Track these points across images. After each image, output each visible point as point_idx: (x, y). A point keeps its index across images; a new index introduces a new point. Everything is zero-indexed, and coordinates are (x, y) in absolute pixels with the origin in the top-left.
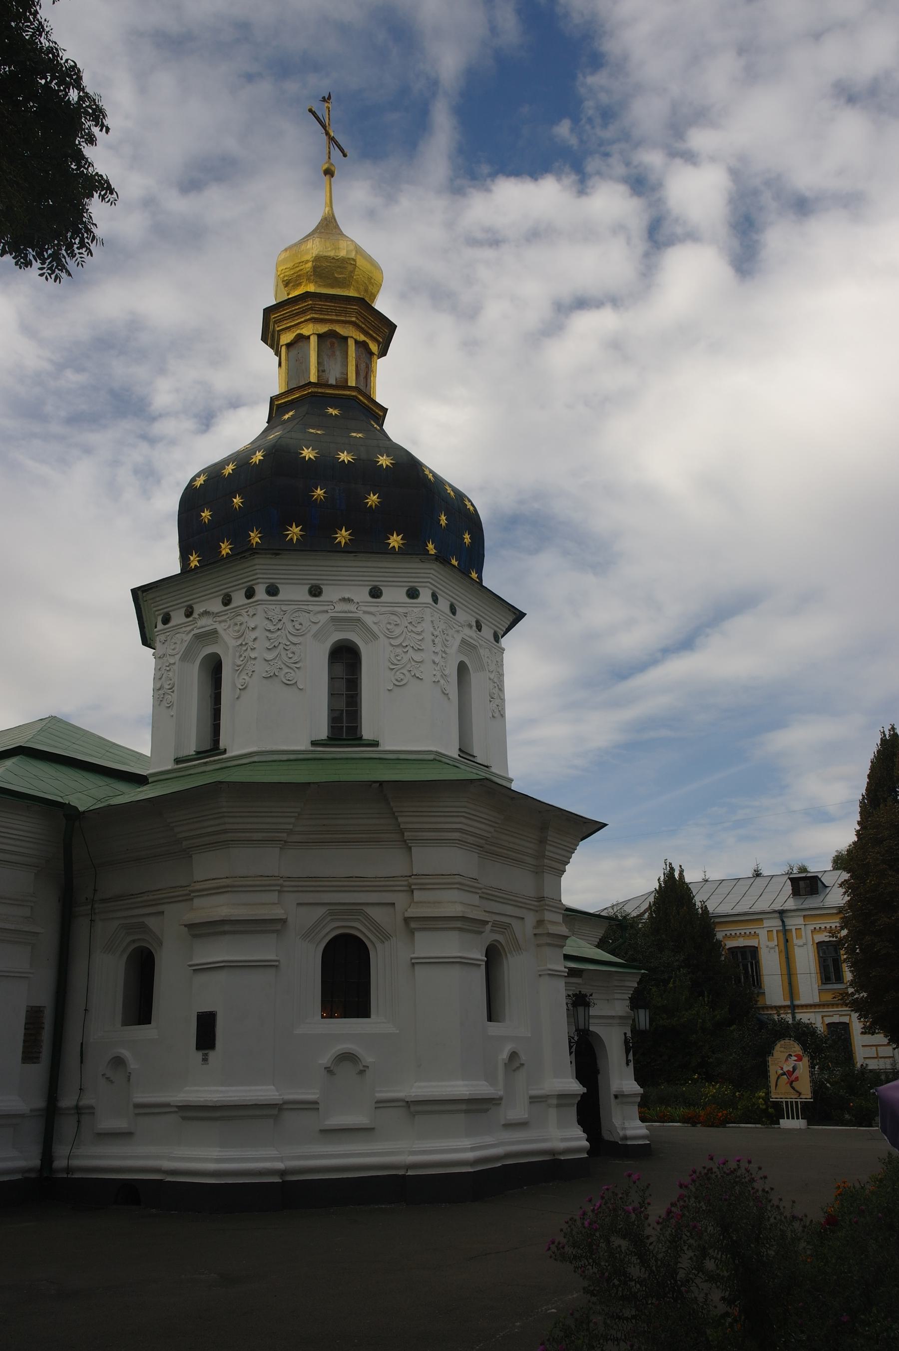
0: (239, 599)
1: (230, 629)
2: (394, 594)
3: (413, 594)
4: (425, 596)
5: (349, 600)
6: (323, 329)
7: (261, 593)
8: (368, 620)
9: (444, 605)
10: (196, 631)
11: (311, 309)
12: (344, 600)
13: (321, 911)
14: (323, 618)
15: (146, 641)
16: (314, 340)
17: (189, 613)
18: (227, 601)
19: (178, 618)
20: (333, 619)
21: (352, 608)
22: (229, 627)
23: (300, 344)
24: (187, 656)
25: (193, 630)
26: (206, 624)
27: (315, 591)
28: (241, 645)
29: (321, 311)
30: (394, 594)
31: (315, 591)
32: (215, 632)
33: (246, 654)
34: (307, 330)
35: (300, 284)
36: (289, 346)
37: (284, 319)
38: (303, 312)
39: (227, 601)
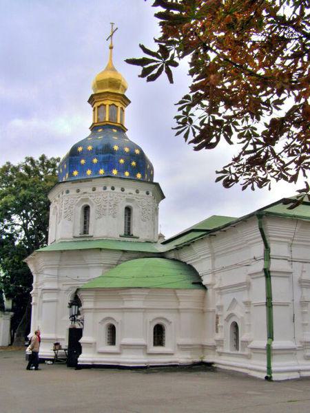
2: (100, 189)
3: (105, 188)
4: (109, 189)
5: (85, 193)
8: (90, 198)
9: (118, 190)
12: (85, 193)
13: (69, 286)
14: (80, 199)
15: (49, 203)
20: (82, 199)
21: (87, 195)
27: (78, 191)
30: (100, 189)
31: (78, 191)
36: (98, 107)
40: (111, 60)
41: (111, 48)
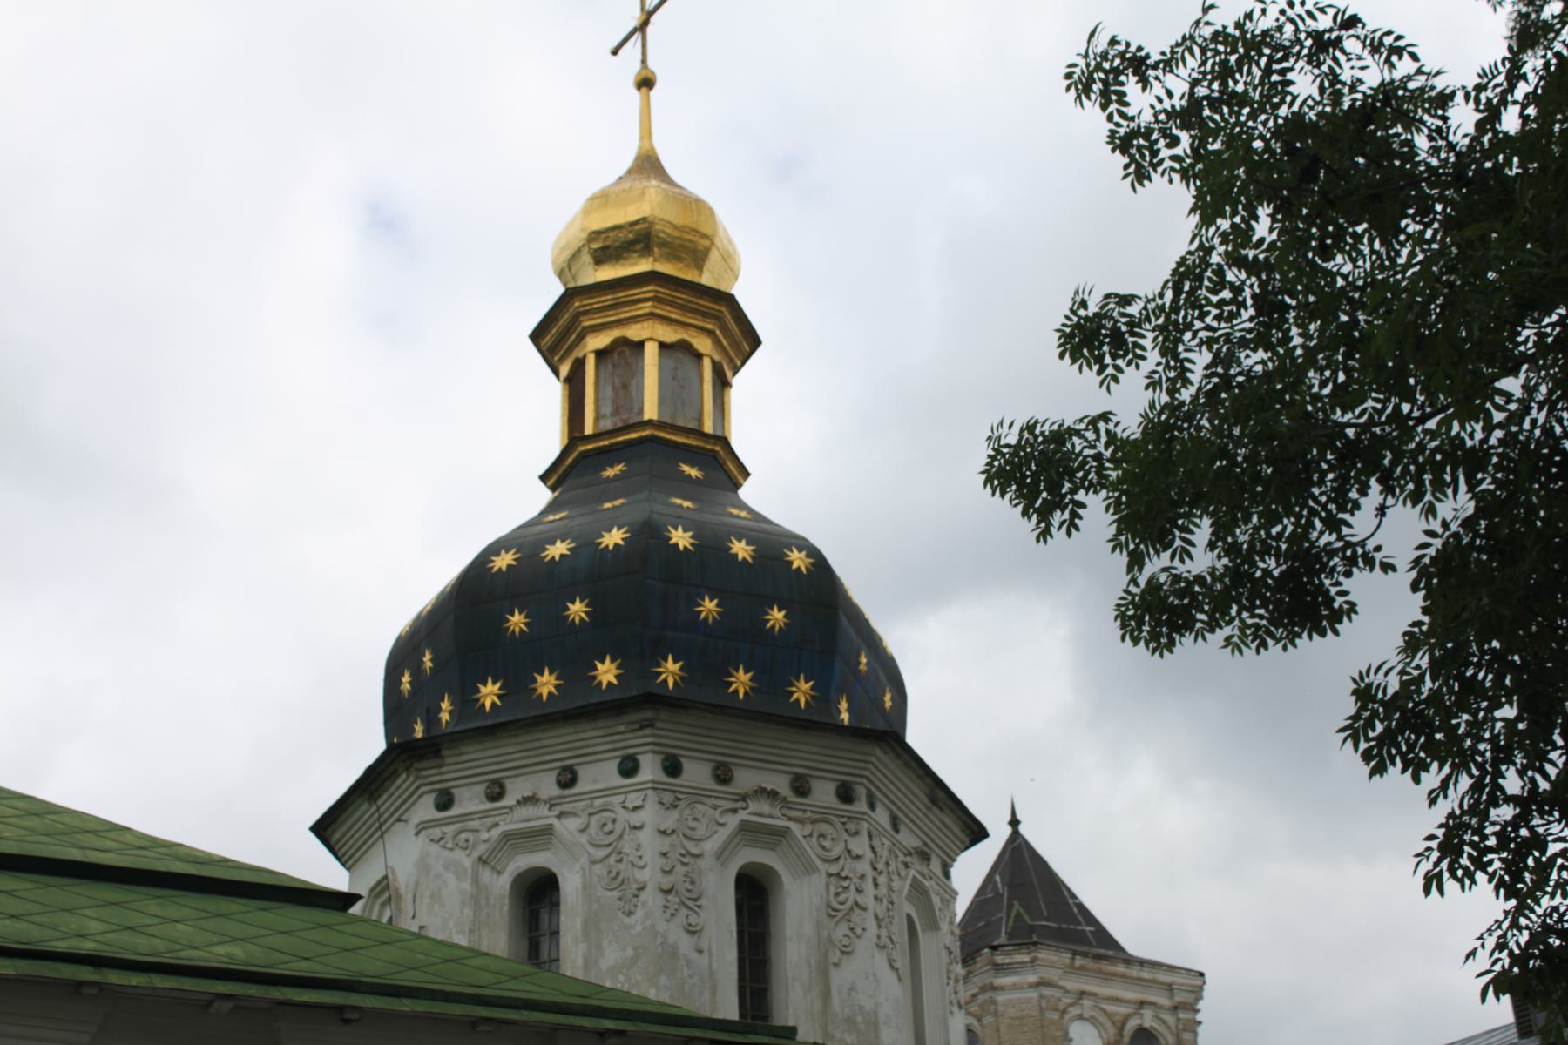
0: (824, 793)
1: (814, 840)
6: (717, 358)
7: (861, 806)
10: (743, 815)
11: (717, 318)
16: (707, 363)
17: (723, 776)
18: (801, 787)
19: (696, 773)
22: (811, 835)
23: (680, 355)
24: (722, 855)
25: (735, 811)
26: (761, 812)
28: (838, 875)
29: (724, 328)
32: (783, 833)
33: (852, 894)
34: (703, 344)
35: (679, 259)
37: (672, 304)
38: (705, 315)
39: (801, 787)
40: (646, 131)
41: (646, 83)
